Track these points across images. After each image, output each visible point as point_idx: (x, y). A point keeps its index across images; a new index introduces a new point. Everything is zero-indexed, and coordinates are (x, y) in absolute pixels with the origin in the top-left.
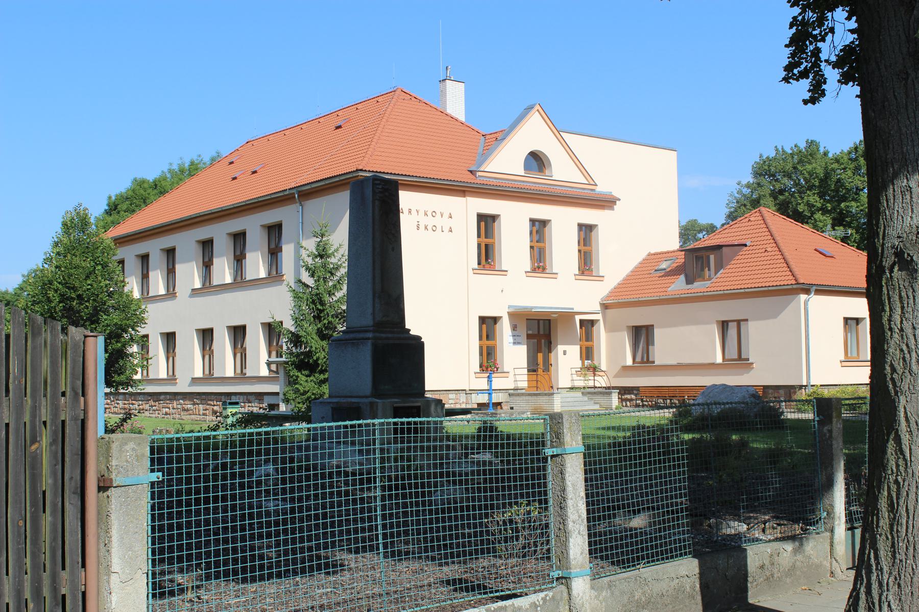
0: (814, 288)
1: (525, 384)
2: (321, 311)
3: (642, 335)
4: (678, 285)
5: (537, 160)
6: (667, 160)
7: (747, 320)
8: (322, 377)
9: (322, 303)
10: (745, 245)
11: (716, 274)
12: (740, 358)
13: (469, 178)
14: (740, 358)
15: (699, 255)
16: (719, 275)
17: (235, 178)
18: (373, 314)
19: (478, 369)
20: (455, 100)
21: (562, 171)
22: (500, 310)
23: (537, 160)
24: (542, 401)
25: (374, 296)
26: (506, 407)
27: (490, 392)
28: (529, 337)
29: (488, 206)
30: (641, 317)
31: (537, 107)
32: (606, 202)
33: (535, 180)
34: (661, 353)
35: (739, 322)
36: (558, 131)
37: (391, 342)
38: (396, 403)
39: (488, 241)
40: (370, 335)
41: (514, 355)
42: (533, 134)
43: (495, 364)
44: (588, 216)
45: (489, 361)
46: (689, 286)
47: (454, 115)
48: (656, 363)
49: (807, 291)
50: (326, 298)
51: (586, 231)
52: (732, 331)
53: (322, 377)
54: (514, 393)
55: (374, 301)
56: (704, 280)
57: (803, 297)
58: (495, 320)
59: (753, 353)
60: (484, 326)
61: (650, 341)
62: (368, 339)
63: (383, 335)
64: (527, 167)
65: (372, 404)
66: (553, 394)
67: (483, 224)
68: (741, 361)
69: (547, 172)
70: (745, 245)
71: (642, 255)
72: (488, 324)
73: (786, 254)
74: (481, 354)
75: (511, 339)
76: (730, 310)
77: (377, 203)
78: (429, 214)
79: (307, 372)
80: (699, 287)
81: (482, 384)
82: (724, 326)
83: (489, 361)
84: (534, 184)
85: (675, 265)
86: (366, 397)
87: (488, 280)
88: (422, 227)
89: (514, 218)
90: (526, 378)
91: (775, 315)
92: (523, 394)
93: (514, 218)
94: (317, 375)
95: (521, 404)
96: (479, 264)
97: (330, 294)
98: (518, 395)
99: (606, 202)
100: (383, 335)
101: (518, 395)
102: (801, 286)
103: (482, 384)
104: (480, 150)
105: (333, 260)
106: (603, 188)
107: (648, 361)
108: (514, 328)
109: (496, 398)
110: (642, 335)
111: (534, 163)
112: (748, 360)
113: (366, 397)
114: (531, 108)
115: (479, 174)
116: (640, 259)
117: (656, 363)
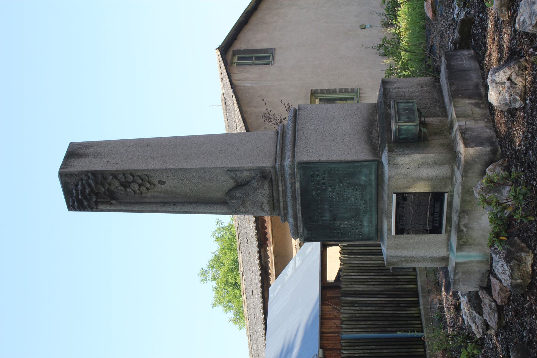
37: (299, 214)
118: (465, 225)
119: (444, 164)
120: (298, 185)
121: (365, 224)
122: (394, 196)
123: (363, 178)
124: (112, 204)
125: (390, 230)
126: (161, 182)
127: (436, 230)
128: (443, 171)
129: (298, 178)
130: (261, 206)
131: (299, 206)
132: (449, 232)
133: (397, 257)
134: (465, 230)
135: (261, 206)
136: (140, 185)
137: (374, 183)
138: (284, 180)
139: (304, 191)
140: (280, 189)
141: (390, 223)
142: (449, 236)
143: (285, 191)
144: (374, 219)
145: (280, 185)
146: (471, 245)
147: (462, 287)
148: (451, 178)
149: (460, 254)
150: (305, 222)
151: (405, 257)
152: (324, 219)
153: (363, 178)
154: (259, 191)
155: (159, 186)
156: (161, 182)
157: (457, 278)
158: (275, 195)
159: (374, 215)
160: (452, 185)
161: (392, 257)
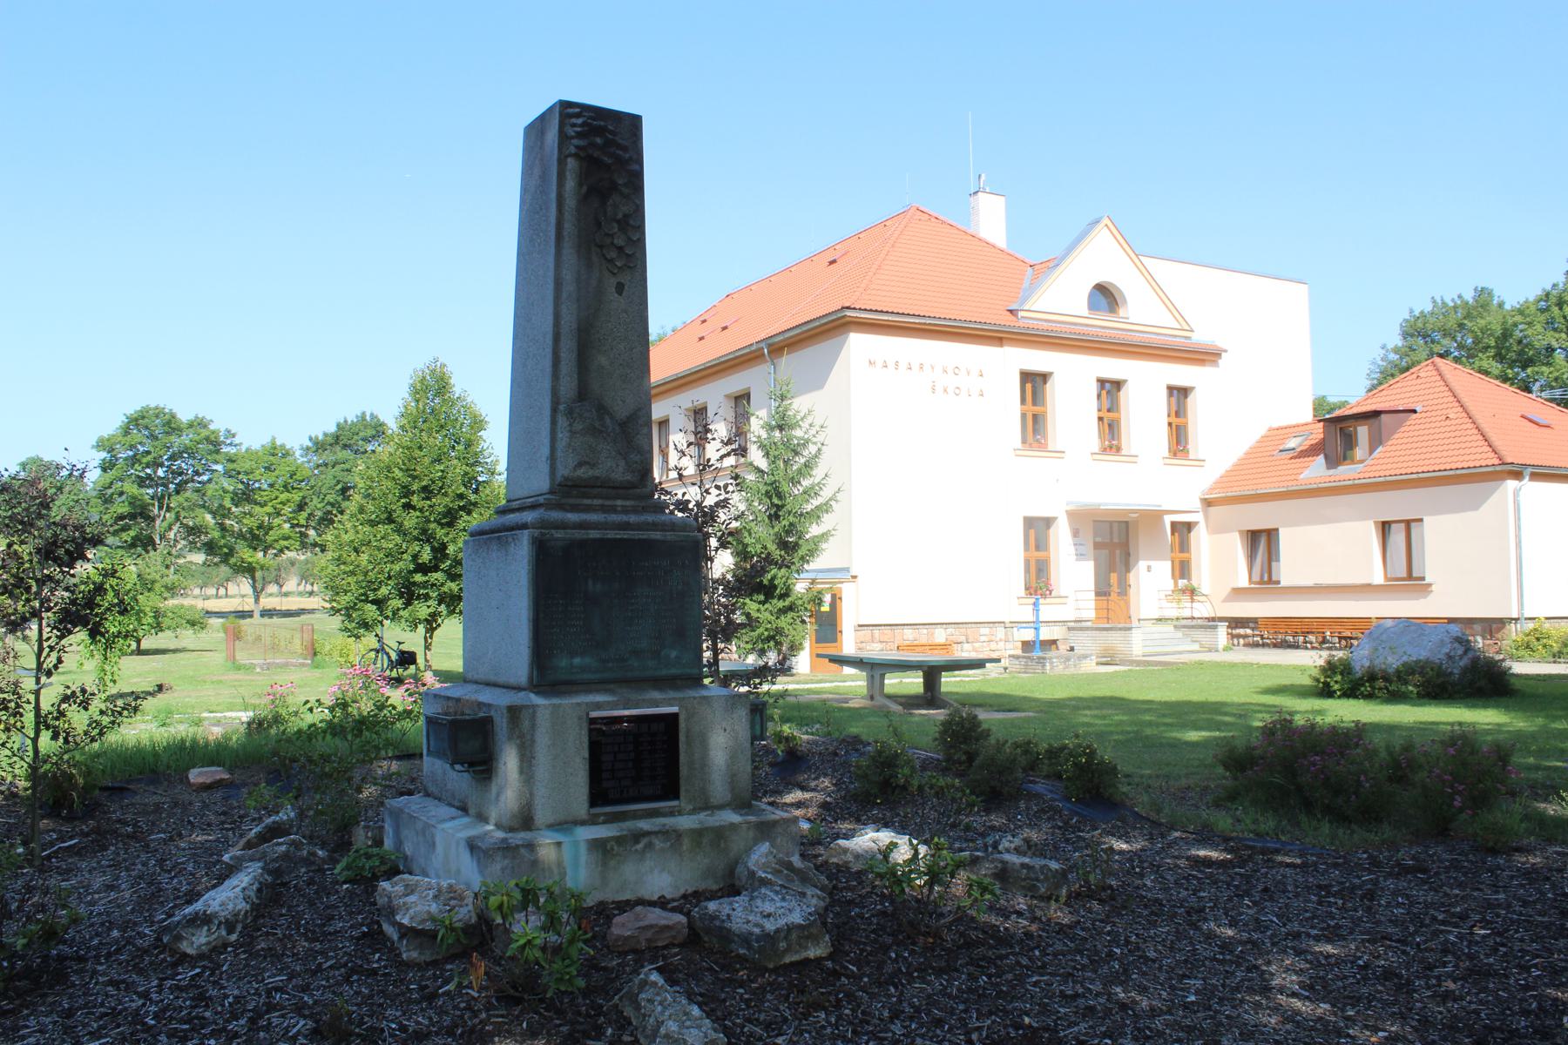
0: (1530, 470)
1: (1091, 614)
2: (779, 508)
3: (1261, 542)
4: (1316, 470)
5: (1105, 296)
6: (1295, 298)
7: (1421, 520)
8: (781, 604)
9: (780, 496)
10: (1414, 411)
11: (1371, 451)
12: (1410, 577)
13: (1007, 320)
14: (1410, 577)
15: (1340, 431)
16: (1375, 454)
17: (701, 339)
18: (552, 458)
19: (1022, 592)
20: (991, 219)
21: (1142, 312)
22: (1055, 507)
23: (1105, 296)
24: (1114, 639)
25: (554, 410)
26: (1063, 647)
27: (1036, 625)
28: (1097, 546)
29: (1037, 360)
30: (1259, 516)
31: (1106, 221)
32: (1206, 356)
33: (1103, 323)
34: (1289, 570)
35: (1408, 523)
36: (1136, 254)
37: (594, 534)
38: (598, 706)
39: (1037, 409)
40: (528, 517)
41: (1075, 574)
42: (1101, 258)
43: (1047, 584)
44: (1181, 374)
45: (1038, 581)
46: (1332, 472)
47: (991, 241)
48: (1283, 584)
49: (1517, 475)
50: (785, 487)
51: (1179, 394)
52: (1398, 537)
53: (781, 604)
54: (1076, 626)
55: (554, 422)
56: (1353, 462)
57: (1511, 484)
58: (1048, 522)
59: (1432, 567)
60: (1032, 532)
61: (1272, 554)
62: (524, 526)
63: (573, 517)
64: (1092, 306)
65: (514, 712)
66: (1130, 629)
67: (1029, 386)
68: (1411, 581)
69: (1122, 312)
70: (1414, 411)
71: (1261, 431)
72: (1037, 529)
73: (1480, 421)
74: (1027, 570)
75: (1072, 550)
76: (1396, 505)
77: (571, 163)
78: (950, 370)
79: (762, 597)
80: (1345, 472)
81: (1027, 614)
82: (1385, 527)
83: (1038, 581)
84: (1105, 331)
85: (1309, 443)
86: (518, 689)
87: (1036, 464)
88: (939, 389)
89: (1074, 378)
90: (1092, 604)
91: (1476, 507)
92: (1087, 629)
93: (1074, 378)
94: (775, 601)
95: (1086, 643)
96: (1024, 441)
97: (794, 482)
98: (1081, 629)
99: (1206, 356)
100: (573, 517)
101: (1081, 629)
102: (1509, 468)
103: (1027, 614)
104: (1026, 284)
105: (798, 433)
106: (1202, 336)
107: (1270, 581)
108: (1076, 533)
109: (1046, 634)
110: (1261, 542)
111: (1103, 301)
112: (1423, 579)
113: (518, 689)
114: (1097, 222)
115: (1021, 314)
116: (1257, 437)
117: (1283, 584)
118: (650, 846)
119: (733, 790)
120: (657, 535)
121: (577, 661)
122: (675, 709)
123: (674, 654)
124: (580, 185)
125: (598, 706)
126: (620, 288)
127: (598, 797)
128: (719, 789)
129: (670, 536)
130: (586, 463)
131: (611, 535)
132: (592, 821)
133: (533, 726)
134: (639, 846)
135: (586, 463)
136: (620, 249)
137: (664, 672)
138: (635, 510)
139: (647, 546)
140: (619, 502)
141: (614, 706)
142: (583, 823)
143: (613, 510)
144: (586, 676)
145: (628, 503)
146: (604, 864)
147: (499, 867)
148: (707, 807)
149: (583, 849)
150: (583, 544)
151: (533, 741)
152: (590, 582)
153: (674, 654)
154: (622, 463)
155: (613, 281)
156: (620, 288)
157: (522, 851)
158: (596, 491)
159: (598, 676)
160: (694, 811)
161: (533, 717)
